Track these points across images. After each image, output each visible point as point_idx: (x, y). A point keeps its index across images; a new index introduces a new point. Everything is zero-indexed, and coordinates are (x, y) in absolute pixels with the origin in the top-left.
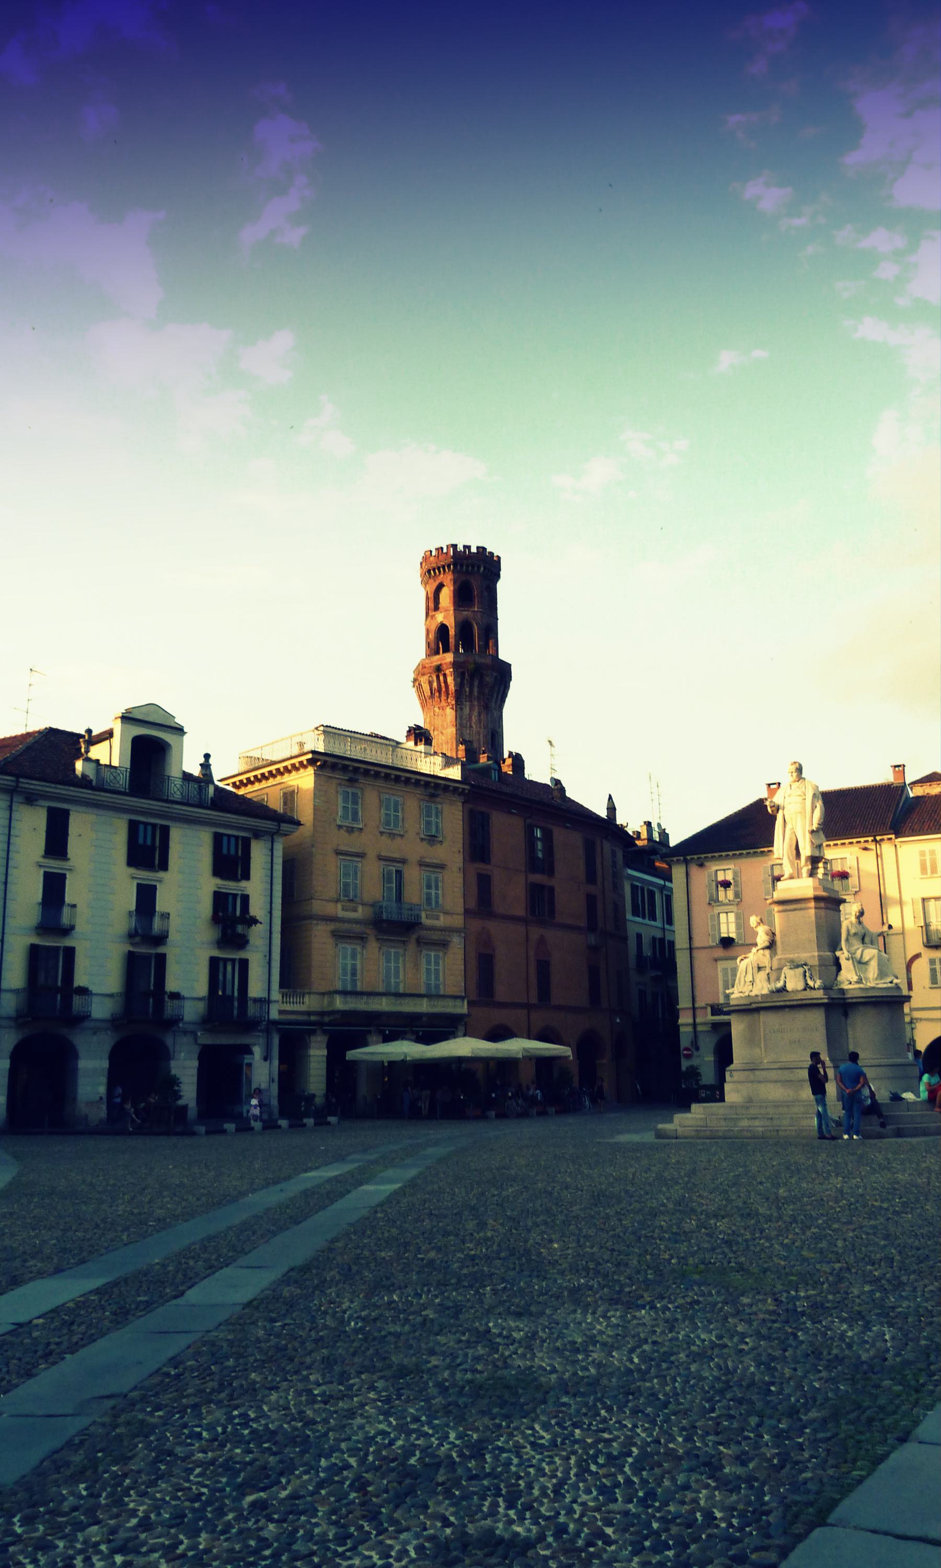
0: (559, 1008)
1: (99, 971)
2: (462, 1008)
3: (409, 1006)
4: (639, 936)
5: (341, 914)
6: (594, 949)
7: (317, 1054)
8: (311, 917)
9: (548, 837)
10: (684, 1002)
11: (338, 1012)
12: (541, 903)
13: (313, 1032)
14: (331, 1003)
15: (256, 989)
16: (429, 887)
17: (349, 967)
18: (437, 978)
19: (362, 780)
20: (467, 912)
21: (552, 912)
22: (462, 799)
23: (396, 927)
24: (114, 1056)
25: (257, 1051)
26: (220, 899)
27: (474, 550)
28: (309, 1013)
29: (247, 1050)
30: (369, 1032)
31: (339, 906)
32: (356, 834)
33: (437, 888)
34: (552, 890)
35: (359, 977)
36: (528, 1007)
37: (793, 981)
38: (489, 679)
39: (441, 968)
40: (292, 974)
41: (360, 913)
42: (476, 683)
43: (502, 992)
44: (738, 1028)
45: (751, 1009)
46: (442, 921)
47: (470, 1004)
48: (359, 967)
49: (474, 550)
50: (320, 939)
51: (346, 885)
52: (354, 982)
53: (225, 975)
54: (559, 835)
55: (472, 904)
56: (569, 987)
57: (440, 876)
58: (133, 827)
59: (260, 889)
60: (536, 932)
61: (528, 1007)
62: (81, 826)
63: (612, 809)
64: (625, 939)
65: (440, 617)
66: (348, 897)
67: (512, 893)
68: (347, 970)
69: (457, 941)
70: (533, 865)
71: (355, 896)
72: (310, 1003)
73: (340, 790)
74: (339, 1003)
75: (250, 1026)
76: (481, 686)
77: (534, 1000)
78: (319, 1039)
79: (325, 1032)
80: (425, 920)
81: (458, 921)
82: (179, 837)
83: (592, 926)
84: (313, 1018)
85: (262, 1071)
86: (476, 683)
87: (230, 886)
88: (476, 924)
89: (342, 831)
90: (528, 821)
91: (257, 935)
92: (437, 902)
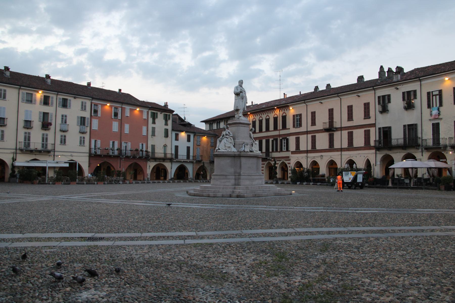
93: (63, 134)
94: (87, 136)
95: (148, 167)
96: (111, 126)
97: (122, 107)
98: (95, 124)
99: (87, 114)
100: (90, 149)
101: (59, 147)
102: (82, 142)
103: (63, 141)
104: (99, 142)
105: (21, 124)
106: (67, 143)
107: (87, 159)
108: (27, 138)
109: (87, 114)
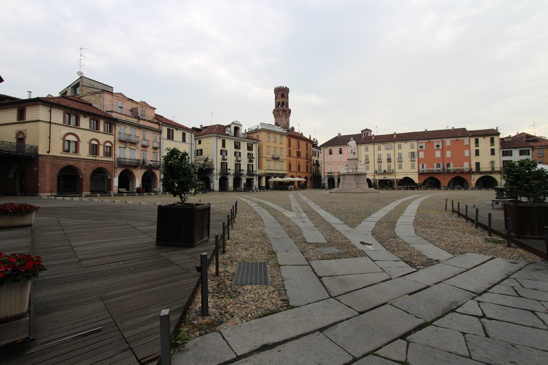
1: (231, 166)
2: (286, 172)
3: (278, 172)
6: (307, 162)
7: (264, 179)
12: (299, 154)
15: (254, 169)
23: (276, 159)
24: (234, 180)
25: (255, 179)
26: (249, 154)
29: (253, 179)
37: (351, 171)
38: (287, 112)
40: (259, 167)
41: (271, 156)
43: (292, 170)
44: (341, 178)
45: (344, 175)
50: (264, 160)
53: (250, 167)
56: (303, 169)
58: (235, 142)
59: (254, 152)
60: (298, 159)
62: (227, 141)
63: (310, 137)
66: (268, 153)
67: (294, 154)
68: (269, 166)
69: (285, 161)
72: (263, 172)
74: (268, 172)
75: (253, 175)
81: (286, 158)
82: (242, 143)
83: (307, 159)
85: (256, 183)
87: (250, 152)
88: (289, 158)
91: (254, 160)
93: (400, 163)
94: (416, 163)
95: (472, 179)
96: (425, 155)
97: (442, 141)
98: (422, 155)
99: (415, 150)
100: (419, 170)
101: (397, 170)
102: (413, 167)
103: (400, 167)
104: (425, 165)
105: (376, 161)
106: (403, 167)
107: (417, 176)
108: (380, 167)
109: (415, 150)
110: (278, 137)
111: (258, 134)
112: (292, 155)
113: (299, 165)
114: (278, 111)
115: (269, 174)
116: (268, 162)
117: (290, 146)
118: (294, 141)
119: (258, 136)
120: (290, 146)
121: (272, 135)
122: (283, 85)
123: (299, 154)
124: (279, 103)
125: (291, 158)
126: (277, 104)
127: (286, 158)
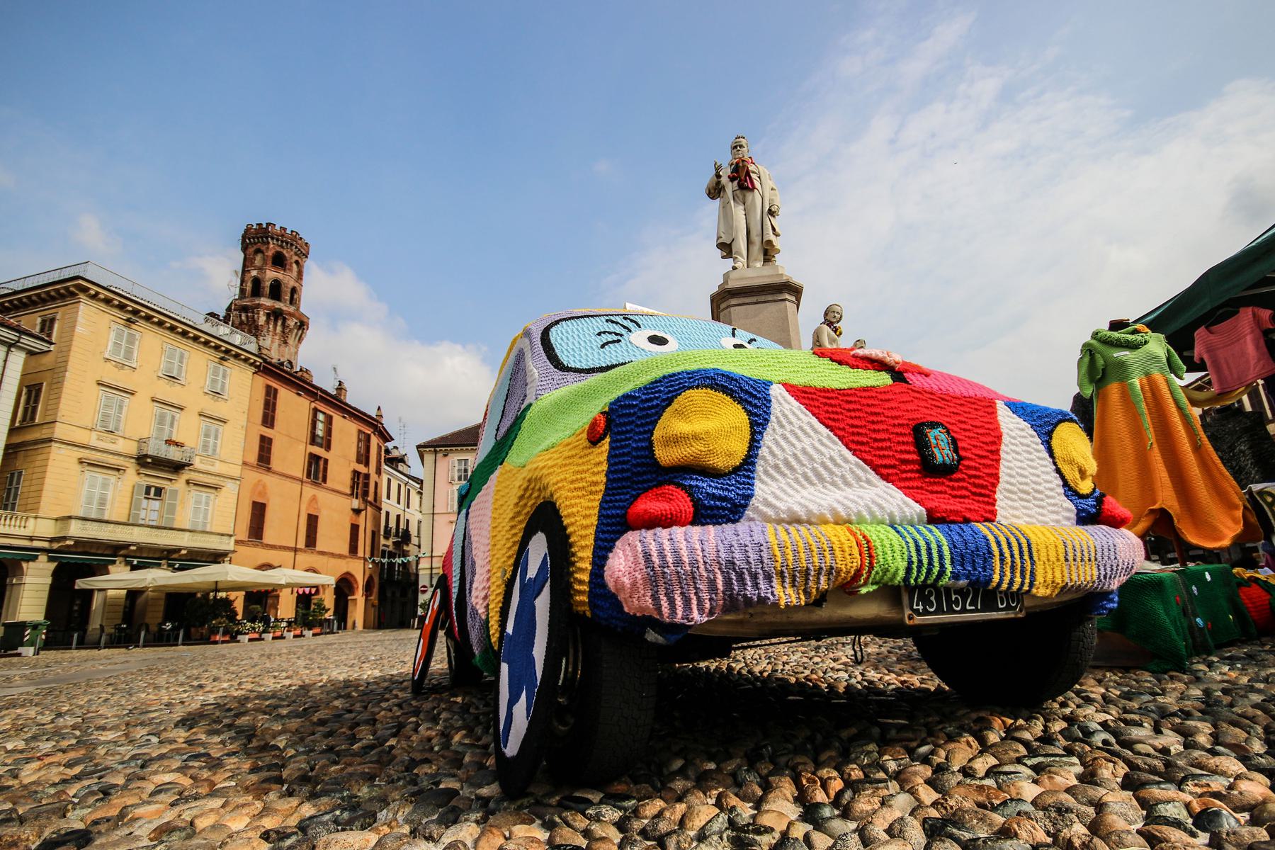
0: (323, 553)
4: (388, 513)
5: (94, 442)
6: (357, 512)
8: (50, 440)
9: (329, 420)
10: (425, 549)
11: (70, 538)
12: (316, 469)
13: (34, 558)
14: (67, 528)
16: (207, 435)
17: (97, 497)
18: (205, 517)
19: (141, 323)
20: (245, 463)
21: (325, 480)
22: (253, 369)
27: (288, 231)
28: (31, 539)
30: (114, 562)
31: (94, 434)
32: (127, 371)
33: (216, 438)
34: (326, 461)
35: (108, 506)
36: (296, 550)
38: (292, 322)
39: (210, 508)
42: (280, 323)
43: (269, 535)
46: (218, 468)
47: (237, 542)
48: (109, 497)
49: (288, 231)
51: (106, 416)
52: (102, 510)
54: (338, 419)
55: (253, 458)
56: (333, 536)
57: (221, 429)
60: (309, 491)
61: (296, 550)
64: (380, 509)
65: (254, 273)
70: (313, 440)
71: (117, 429)
73: (114, 326)
74: (76, 530)
76: (283, 325)
77: (301, 545)
78: (41, 566)
79: (51, 559)
80: (197, 463)
81: (236, 471)
84: (36, 544)
86: (280, 323)
88: (254, 476)
89: (109, 365)
90: (313, 405)
92: (214, 450)
110: (198, 361)
111: (49, 310)
112: (275, 463)
113: (313, 521)
114: (245, 309)
115: (84, 545)
116: (99, 476)
117: (268, 420)
118: (293, 407)
119: (48, 325)
120: (268, 420)
121: (150, 341)
122: (283, 220)
123: (316, 469)
124: (257, 282)
125: (268, 479)
126: (249, 286)
127: (236, 471)
